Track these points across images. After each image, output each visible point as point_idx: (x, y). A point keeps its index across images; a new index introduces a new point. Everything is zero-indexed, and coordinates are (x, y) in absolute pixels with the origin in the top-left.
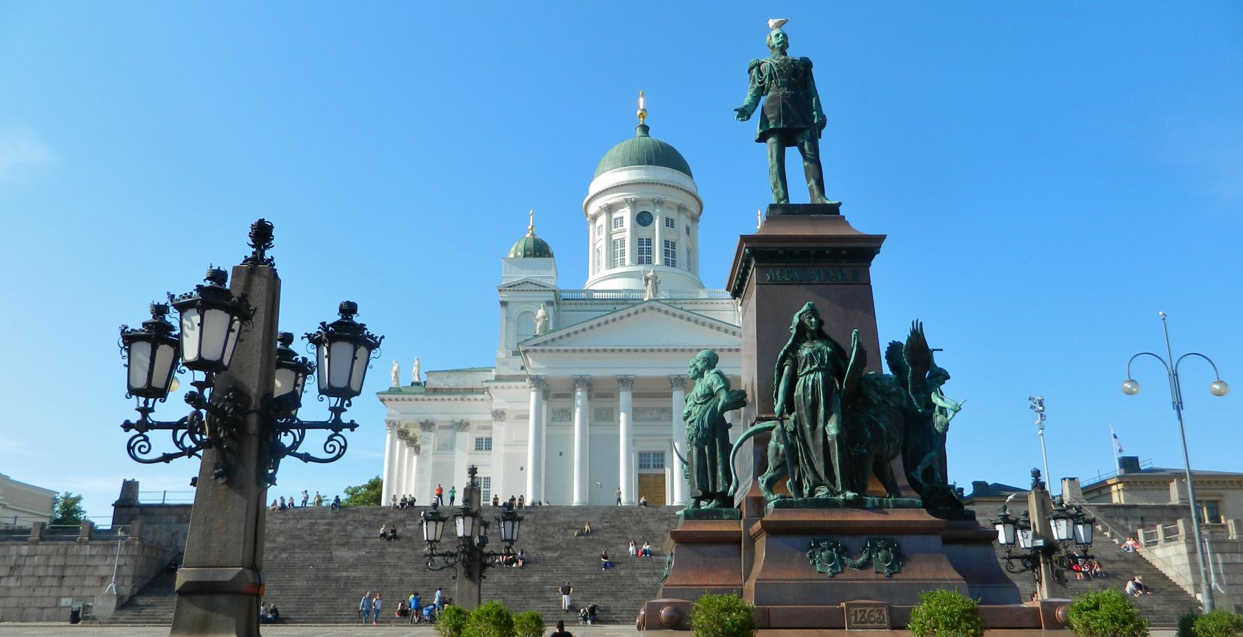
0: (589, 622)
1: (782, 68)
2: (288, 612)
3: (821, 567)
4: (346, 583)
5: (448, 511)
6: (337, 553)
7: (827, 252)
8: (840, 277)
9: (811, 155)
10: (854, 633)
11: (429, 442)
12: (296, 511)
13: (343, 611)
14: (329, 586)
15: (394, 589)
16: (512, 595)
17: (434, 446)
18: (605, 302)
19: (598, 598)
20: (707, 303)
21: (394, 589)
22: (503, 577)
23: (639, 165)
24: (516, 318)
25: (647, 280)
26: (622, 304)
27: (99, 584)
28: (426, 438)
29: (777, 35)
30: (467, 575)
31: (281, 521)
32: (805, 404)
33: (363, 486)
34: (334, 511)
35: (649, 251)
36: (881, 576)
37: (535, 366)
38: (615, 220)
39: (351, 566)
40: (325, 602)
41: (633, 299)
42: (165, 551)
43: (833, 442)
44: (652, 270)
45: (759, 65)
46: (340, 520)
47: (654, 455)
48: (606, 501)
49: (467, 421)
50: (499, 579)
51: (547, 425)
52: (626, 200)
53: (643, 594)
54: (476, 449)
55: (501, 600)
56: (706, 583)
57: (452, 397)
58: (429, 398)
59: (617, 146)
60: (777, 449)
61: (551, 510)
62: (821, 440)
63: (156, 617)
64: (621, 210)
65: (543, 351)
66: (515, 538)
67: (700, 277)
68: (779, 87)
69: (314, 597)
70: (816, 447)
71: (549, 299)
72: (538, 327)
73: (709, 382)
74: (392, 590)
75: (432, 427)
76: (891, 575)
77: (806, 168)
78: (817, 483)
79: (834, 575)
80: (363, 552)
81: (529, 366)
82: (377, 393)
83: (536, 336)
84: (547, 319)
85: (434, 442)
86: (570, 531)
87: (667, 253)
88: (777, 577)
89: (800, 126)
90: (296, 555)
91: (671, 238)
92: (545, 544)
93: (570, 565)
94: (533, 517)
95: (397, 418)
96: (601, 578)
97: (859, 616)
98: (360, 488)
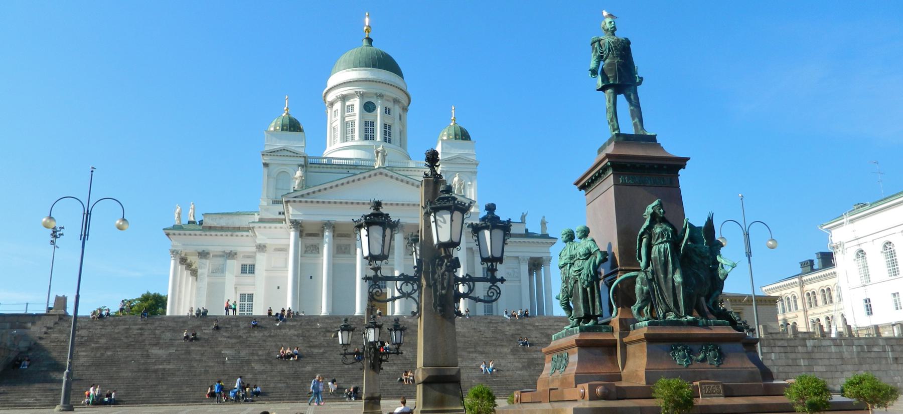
0: (353, 399)
1: (616, 45)
2: (119, 396)
3: (679, 361)
4: (162, 374)
5: (233, 319)
6: (153, 351)
7: (656, 166)
8: (662, 182)
9: (636, 103)
10: (706, 400)
11: (205, 267)
12: (111, 319)
13: (164, 395)
14: (150, 376)
15: (202, 377)
16: (293, 380)
17: (209, 270)
18: (340, 167)
19: (356, 381)
20: (415, 171)
21: (202, 377)
22: (284, 367)
23: (366, 67)
24: (275, 176)
25: (377, 153)
26: (354, 169)
28: (203, 264)
29: (611, 22)
30: (372, 367)
31: (101, 327)
32: (660, 262)
33: (137, 299)
34: (143, 319)
35: (373, 131)
36: (713, 366)
37: (293, 212)
38: (348, 106)
39: (165, 361)
40: (149, 388)
41: (361, 166)
42: (10, 350)
43: (679, 286)
44: (381, 146)
45: (599, 41)
46: (149, 326)
48: (343, 312)
49: (235, 252)
50: (282, 369)
51: (301, 256)
52: (357, 93)
53: (388, 378)
54: (242, 273)
55: (285, 384)
56: (599, 372)
57: (224, 233)
58: (205, 233)
59: (352, 50)
60: (642, 290)
61: (312, 318)
62: (671, 284)
63: (10, 402)
64: (352, 100)
65: (300, 202)
66: (402, 342)
67: (408, 151)
68: (614, 57)
69: (139, 384)
70: (667, 289)
71: (301, 163)
72: (296, 184)
73: (588, 246)
74: (200, 378)
75: (208, 256)
76: (718, 366)
77: (632, 111)
78: (668, 310)
79: (688, 365)
80: (172, 350)
81: (288, 212)
82: (164, 229)
83: (295, 191)
84: (303, 178)
85: (209, 267)
86: (328, 334)
87: (385, 133)
88: (656, 368)
89: (628, 83)
90: (119, 353)
91: (389, 122)
92: (311, 343)
93: (332, 358)
94: (299, 323)
95: (178, 246)
96: (356, 367)
97: (707, 390)
98: (134, 301)
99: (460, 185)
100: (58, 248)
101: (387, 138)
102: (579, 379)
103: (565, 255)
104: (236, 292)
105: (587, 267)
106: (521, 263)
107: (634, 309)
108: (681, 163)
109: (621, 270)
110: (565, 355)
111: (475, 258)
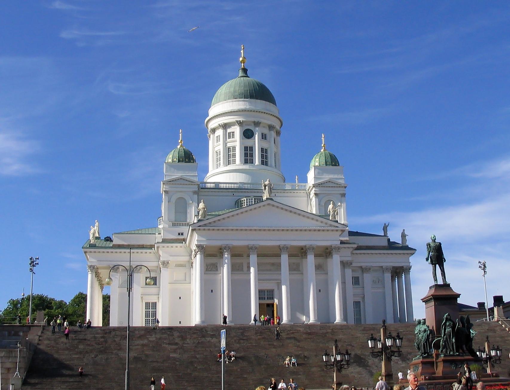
23: (244, 98)
25: (265, 186)
27: (7, 372)
35: (252, 155)
38: (229, 133)
44: (268, 180)
47: (267, 291)
52: (237, 122)
60: (442, 344)
64: (233, 127)
65: (204, 230)
71: (194, 190)
75: (118, 270)
86: (242, 341)
87: (262, 156)
91: (265, 145)
99: (334, 211)
100: (35, 273)
101: (264, 161)
102: (421, 374)
103: (417, 330)
104: (142, 301)
105: (425, 335)
106: (384, 273)
107: (440, 351)
108: (458, 296)
109: (437, 337)
110: (417, 366)
111: (346, 270)
